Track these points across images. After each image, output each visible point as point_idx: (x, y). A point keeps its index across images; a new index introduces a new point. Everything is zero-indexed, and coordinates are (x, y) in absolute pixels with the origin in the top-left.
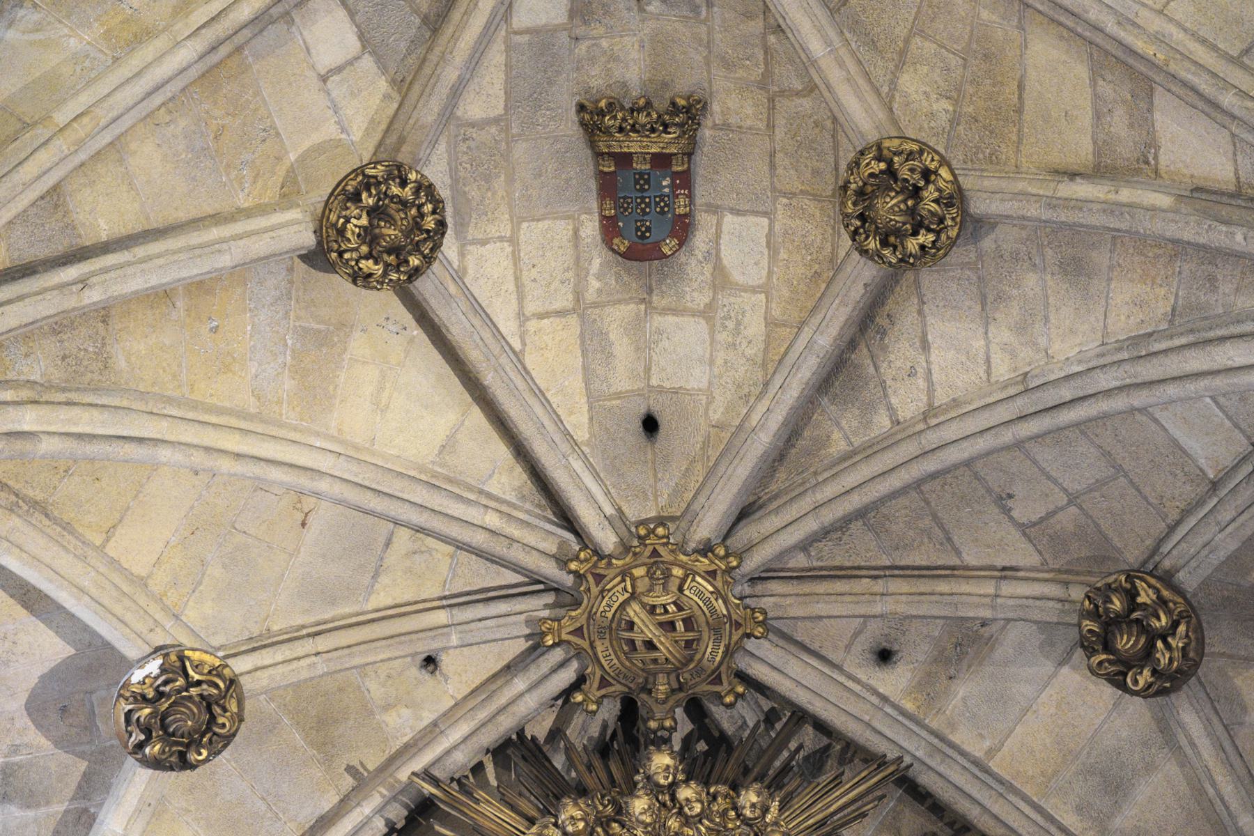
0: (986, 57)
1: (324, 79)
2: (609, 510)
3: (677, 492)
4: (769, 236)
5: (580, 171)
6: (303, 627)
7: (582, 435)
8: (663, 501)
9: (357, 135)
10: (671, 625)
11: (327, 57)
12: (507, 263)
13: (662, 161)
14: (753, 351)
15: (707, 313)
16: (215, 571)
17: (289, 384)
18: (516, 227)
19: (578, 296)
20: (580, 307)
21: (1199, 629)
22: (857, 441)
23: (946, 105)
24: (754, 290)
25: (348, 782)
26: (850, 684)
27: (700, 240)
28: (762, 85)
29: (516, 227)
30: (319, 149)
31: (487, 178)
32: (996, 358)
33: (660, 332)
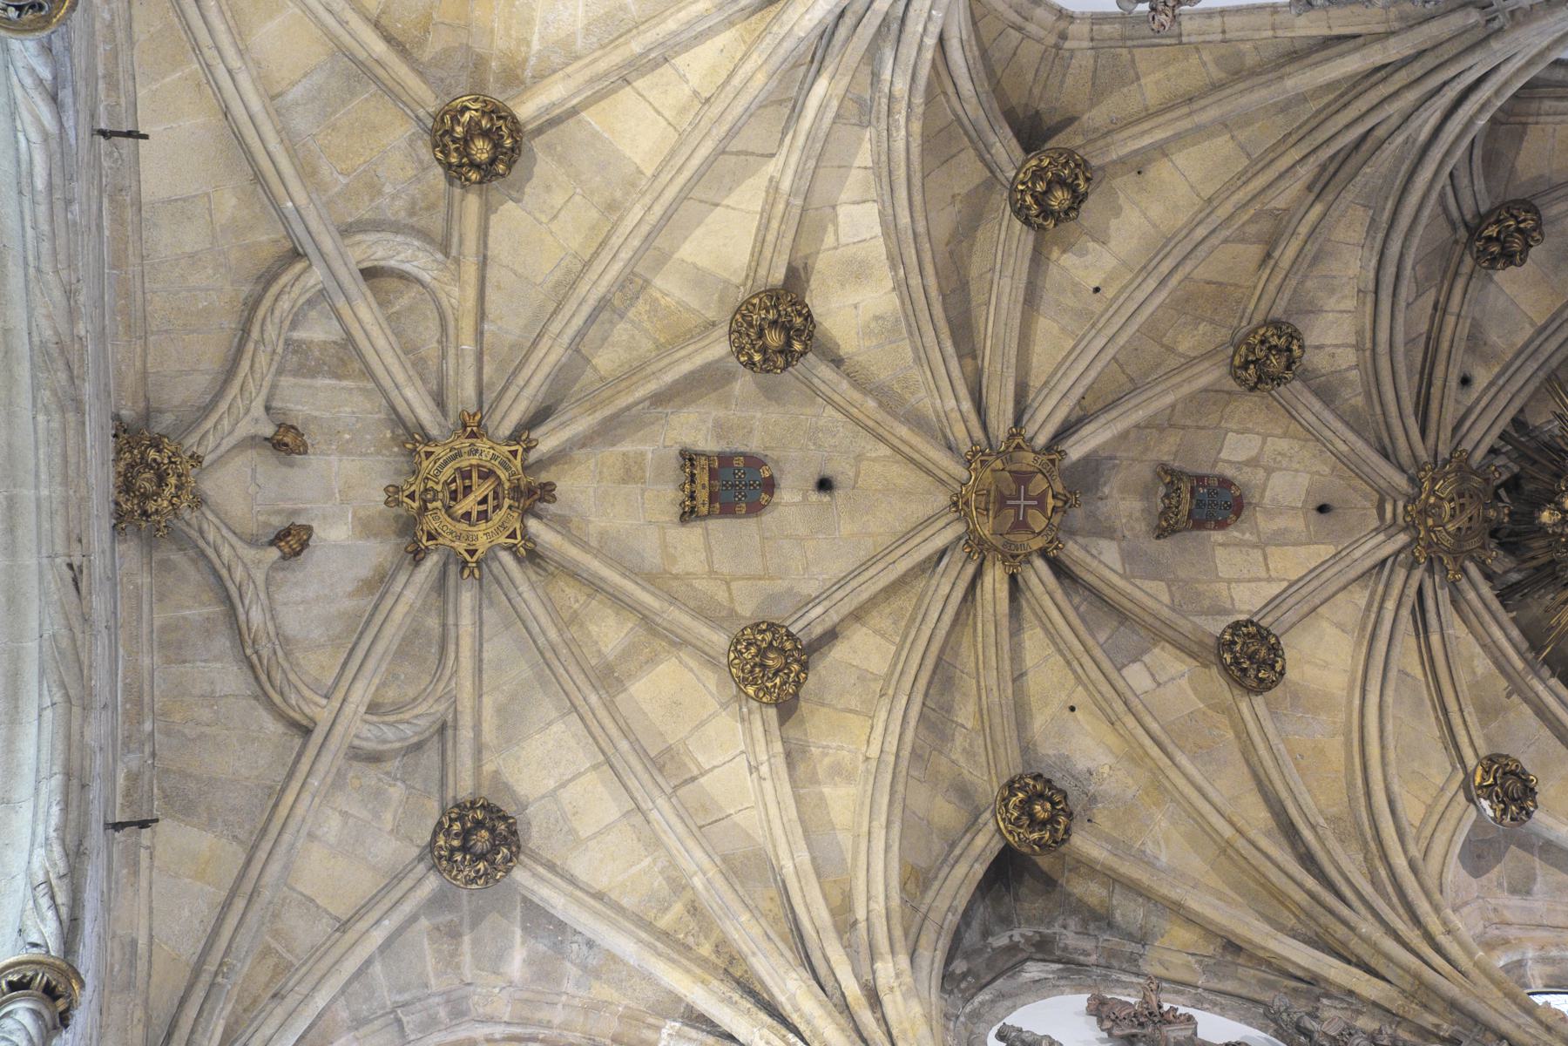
0: (1187, 301)
1: (1159, 685)
2: (1381, 537)
3: (1365, 496)
4: (1237, 432)
5: (1190, 539)
6: (1437, 718)
7: (1332, 550)
8: (1368, 505)
9: (1184, 668)
10: (1462, 505)
11: (1148, 683)
12: (1242, 586)
13: (1193, 491)
14: (1296, 445)
15: (1269, 471)
16: (1416, 765)
17: (1323, 717)
18: (1223, 580)
19: (1255, 546)
20: (1261, 545)
21: (1515, 202)
22: (1360, 389)
23: (1201, 327)
24: (1264, 442)
25: (1515, 698)
26: (1483, 404)
27: (1229, 472)
28: (1161, 429)
29: (1219, 579)
30: (1195, 690)
31: (1199, 594)
32: (1342, 306)
33: (1273, 500)
